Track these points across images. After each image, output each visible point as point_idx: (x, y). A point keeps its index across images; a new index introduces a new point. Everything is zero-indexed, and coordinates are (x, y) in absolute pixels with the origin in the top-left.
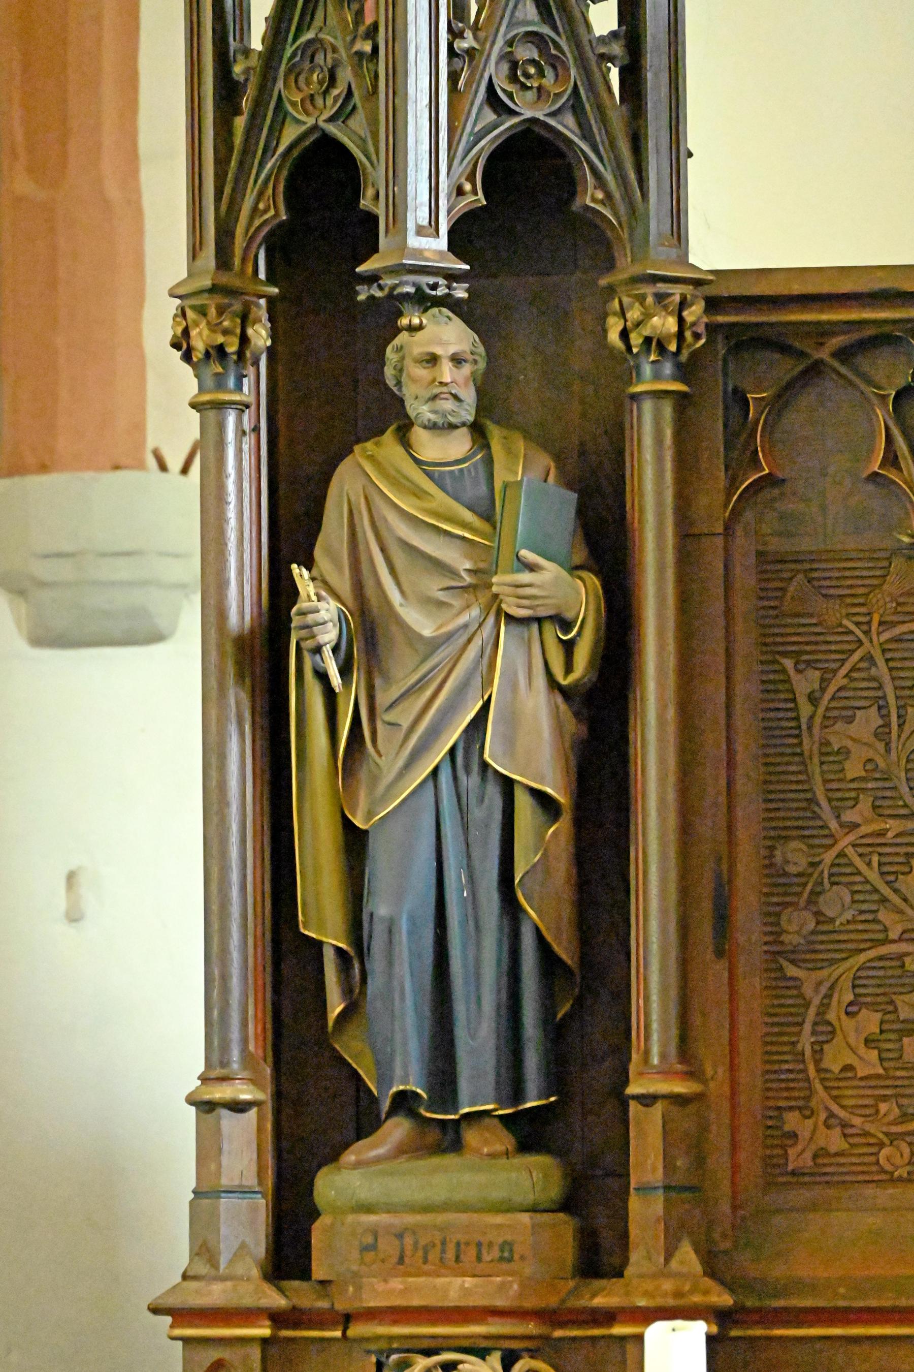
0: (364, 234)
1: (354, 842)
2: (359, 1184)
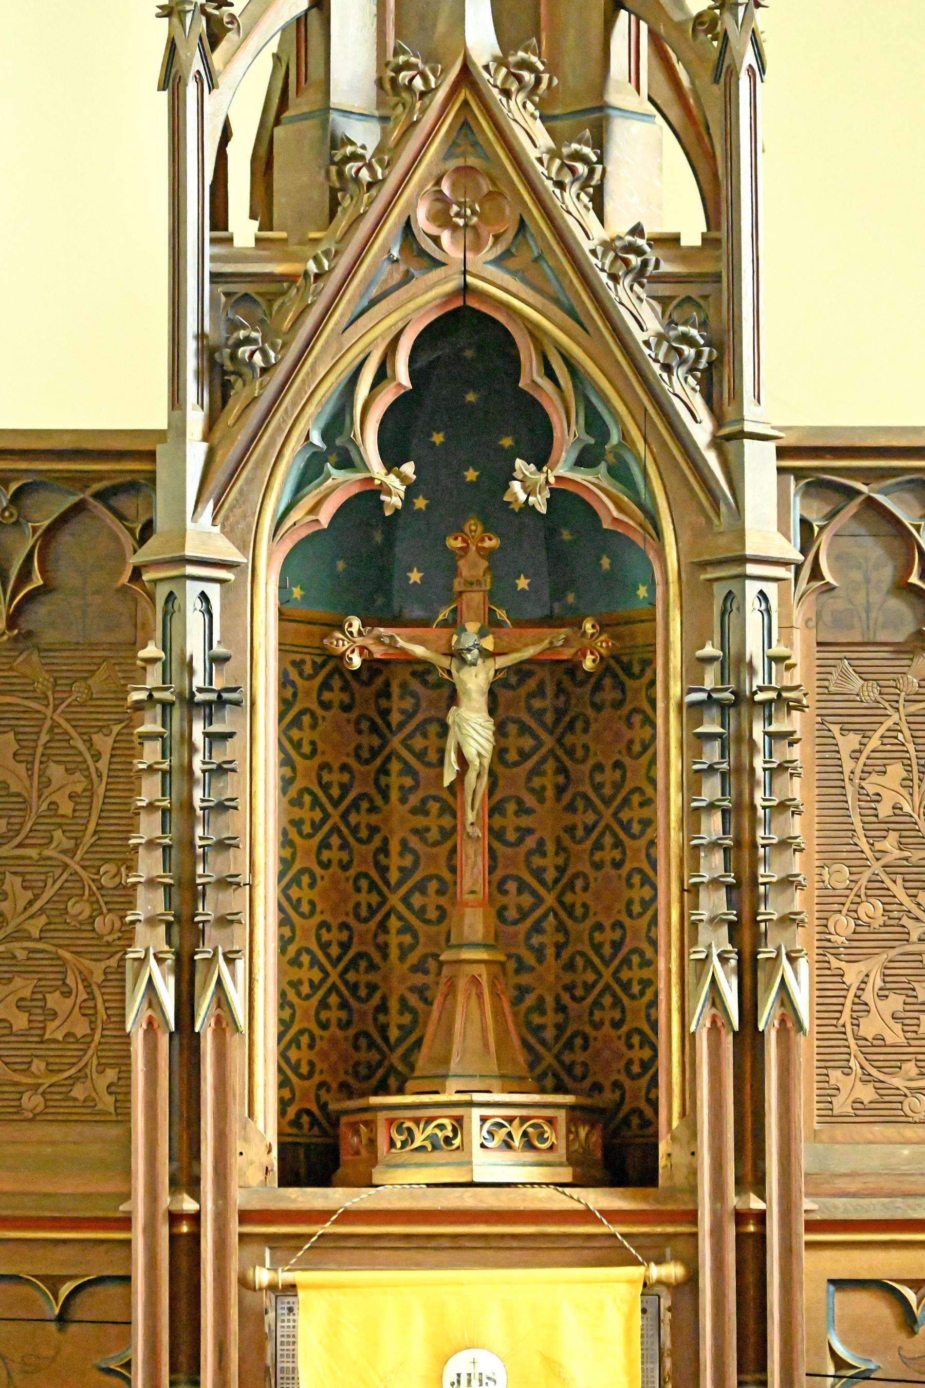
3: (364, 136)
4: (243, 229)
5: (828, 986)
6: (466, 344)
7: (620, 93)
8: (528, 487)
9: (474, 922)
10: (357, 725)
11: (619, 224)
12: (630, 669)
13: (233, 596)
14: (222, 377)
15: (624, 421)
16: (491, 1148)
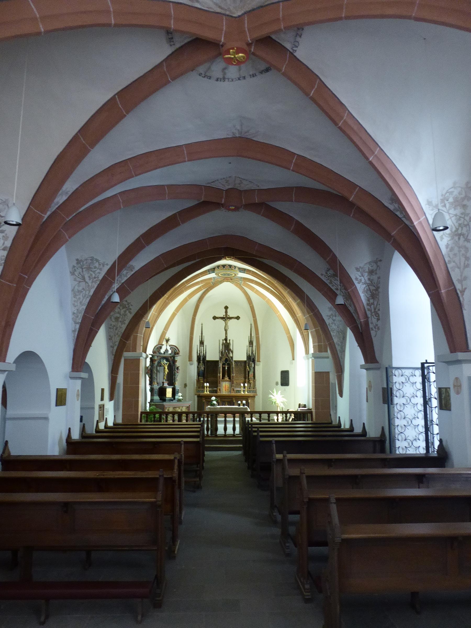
2: (200, 377)
6: (226, 359)
10: (224, 368)
13: (221, 365)
16: (227, 378)
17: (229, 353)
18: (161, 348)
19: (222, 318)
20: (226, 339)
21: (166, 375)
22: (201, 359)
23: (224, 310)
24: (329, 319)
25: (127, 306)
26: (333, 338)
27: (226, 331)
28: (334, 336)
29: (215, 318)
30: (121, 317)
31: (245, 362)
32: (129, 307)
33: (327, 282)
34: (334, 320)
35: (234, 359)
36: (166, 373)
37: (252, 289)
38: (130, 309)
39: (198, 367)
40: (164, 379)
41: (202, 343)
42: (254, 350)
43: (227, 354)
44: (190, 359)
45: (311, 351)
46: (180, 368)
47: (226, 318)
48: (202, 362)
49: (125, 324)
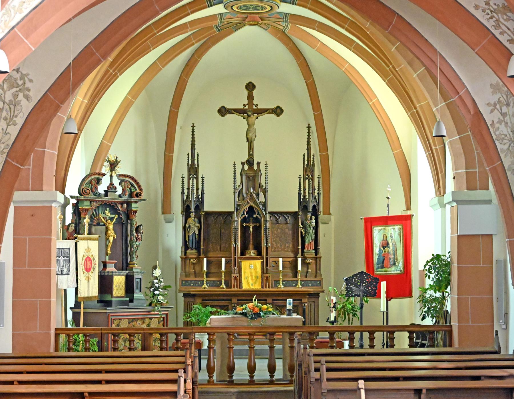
0: (190, 209)
1: (189, 236)
2: (189, 251)
3: (245, 196)
4: (237, 200)
5: (272, 245)
7: (260, 193)
8: (254, 216)
9: (251, 240)
10: (245, 229)
11: (260, 201)
12: (260, 226)
14: (237, 210)
15: (260, 212)
17: (258, 195)
18: (98, 181)
19: (241, 112)
20: (250, 162)
21: (110, 245)
22: (193, 208)
23: (246, 93)
24: (492, 111)
25: (20, 82)
26: (502, 156)
27: (250, 142)
28: (502, 150)
29: (223, 111)
30: (6, 106)
31: (295, 215)
32: (24, 83)
33: (489, 24)
34: (504, 115)
35: (269, 208)
36: (111, 239)
37: (313, 42)
38: (29, 90)
39: (184, 228)
40: (106, 254)
41: (193, 170)
42: (316, 187)
43: (251, 195)
44: (166, 209)
45: (450, 185)
46: (142, 229)
47: (249, 111)
48: (193, 215)
49: (15, 124)
